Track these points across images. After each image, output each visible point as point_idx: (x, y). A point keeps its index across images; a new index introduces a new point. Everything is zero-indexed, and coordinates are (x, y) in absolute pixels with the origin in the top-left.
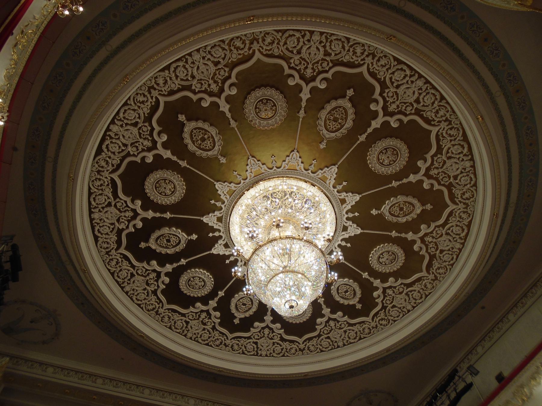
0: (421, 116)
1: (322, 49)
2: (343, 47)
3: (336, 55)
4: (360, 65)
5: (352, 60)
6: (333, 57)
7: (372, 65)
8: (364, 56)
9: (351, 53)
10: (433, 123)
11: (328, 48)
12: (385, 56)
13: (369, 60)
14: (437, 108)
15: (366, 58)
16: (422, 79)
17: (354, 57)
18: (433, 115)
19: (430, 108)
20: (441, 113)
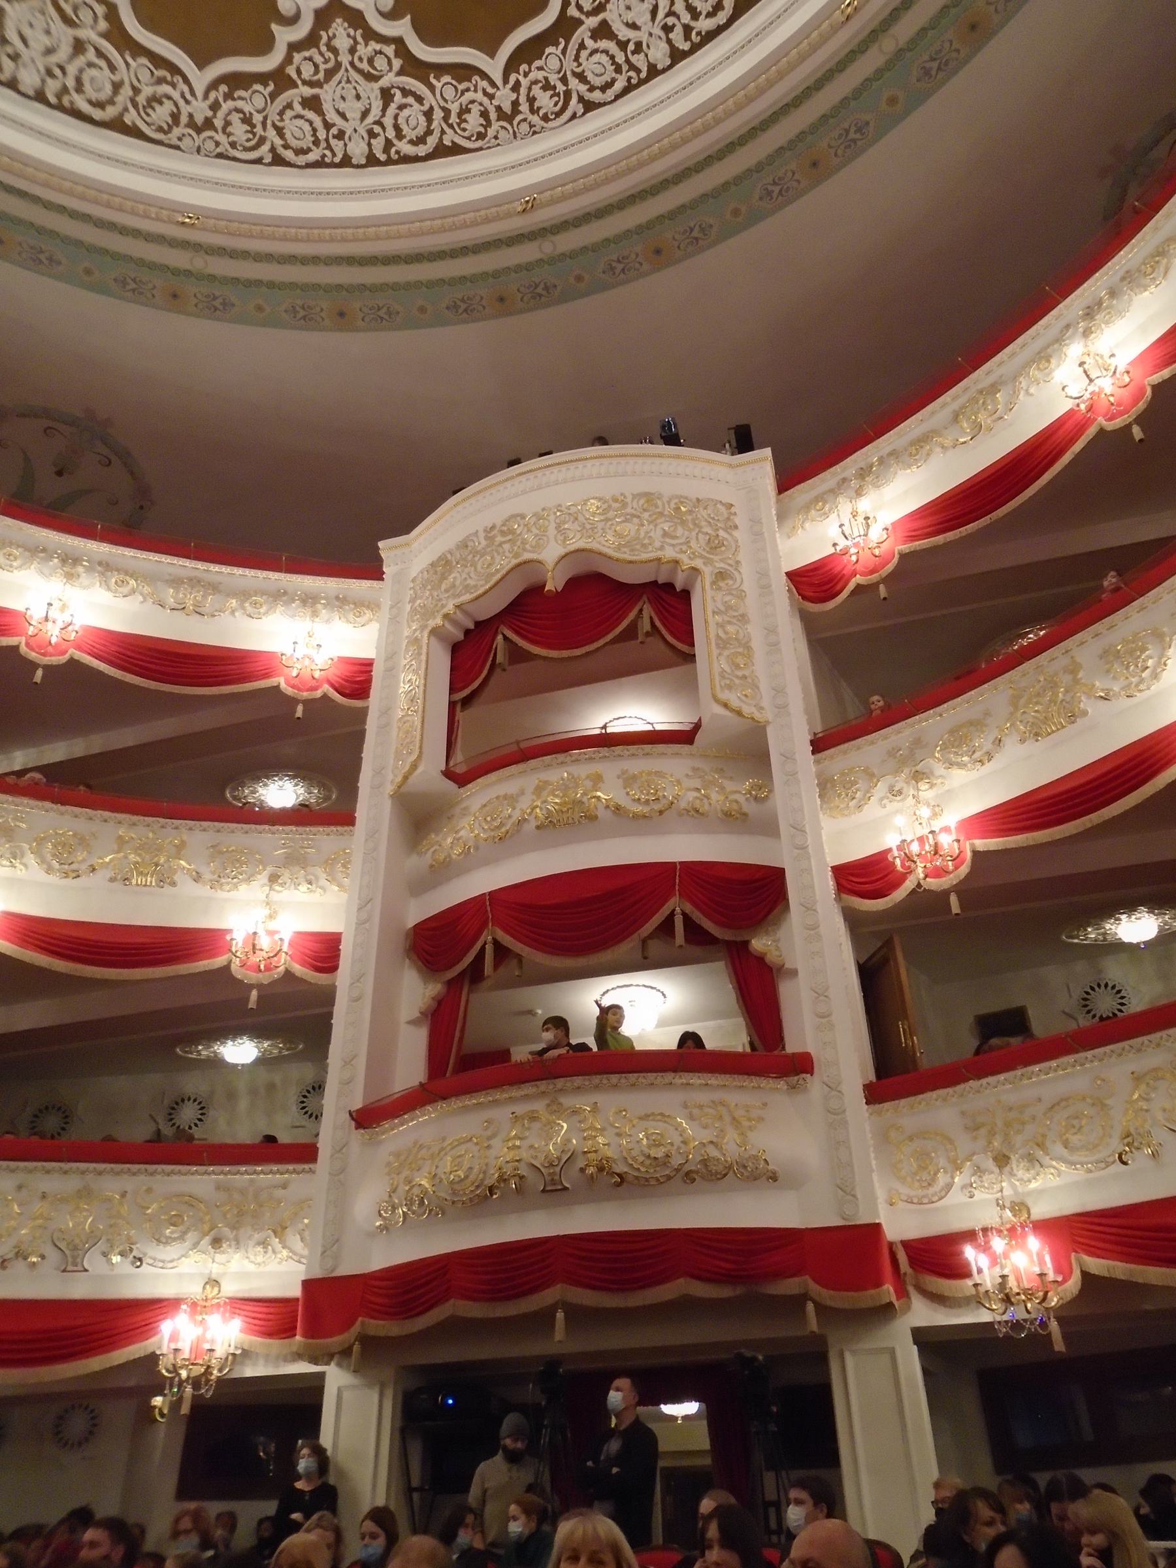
0: (262, 78)
1: (623, 33)
2: (581, 77)
3: (582, 46)
4: (511, 66)
5: (538, 63)
6: (582, 33)
7: (485, 93)
8: (522, 98)
9: (554, 79)
10: (223, 88)
11: (611, 46)
12: (481, 136)
13: (504, 97)
14: (259, 130)
15: (514, 96)
16: (363, 161)
17: (540, 75)
18: (247, 108)
19: (273, 117)
20: (239, 130)
